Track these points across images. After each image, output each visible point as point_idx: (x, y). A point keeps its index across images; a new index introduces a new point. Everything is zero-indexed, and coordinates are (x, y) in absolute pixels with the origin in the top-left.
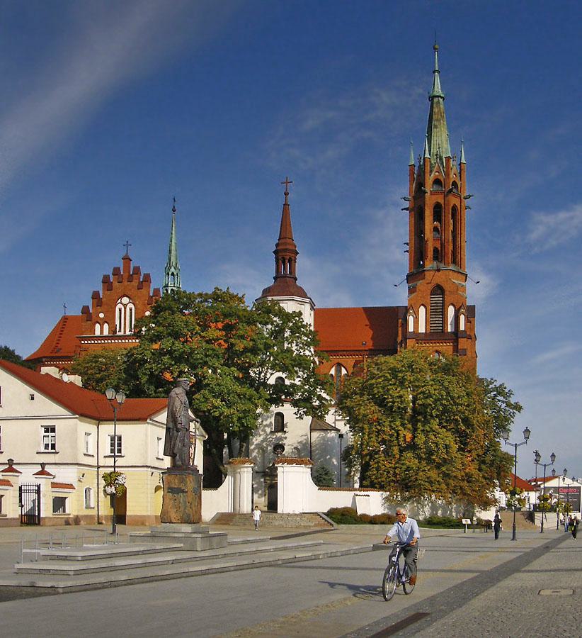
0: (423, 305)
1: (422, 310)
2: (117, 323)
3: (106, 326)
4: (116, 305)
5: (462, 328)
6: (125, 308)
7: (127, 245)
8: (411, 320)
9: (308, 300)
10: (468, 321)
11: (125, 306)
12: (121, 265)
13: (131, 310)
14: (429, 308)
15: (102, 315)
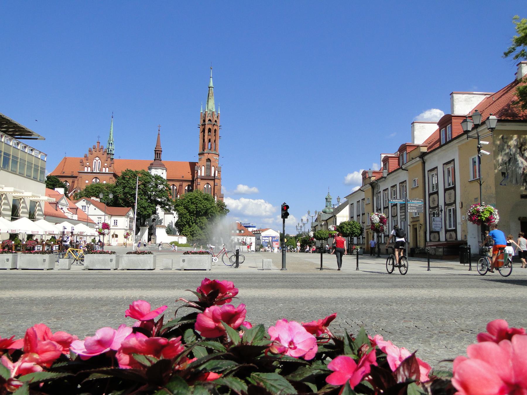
0: (203, 166)
1: (203, 167)
2: (94, 167)
3: (89, 168)
4: (94, 160)
5: (216, 175)
6: (97, 162)
7: (99, 137)
8: (199, 171)
9: (165, 169)
10: (218, 173)
11: (97, 160)
12: (96, 144)
13: (99, 162)
14: (205, 167)
15: (88, 164)
